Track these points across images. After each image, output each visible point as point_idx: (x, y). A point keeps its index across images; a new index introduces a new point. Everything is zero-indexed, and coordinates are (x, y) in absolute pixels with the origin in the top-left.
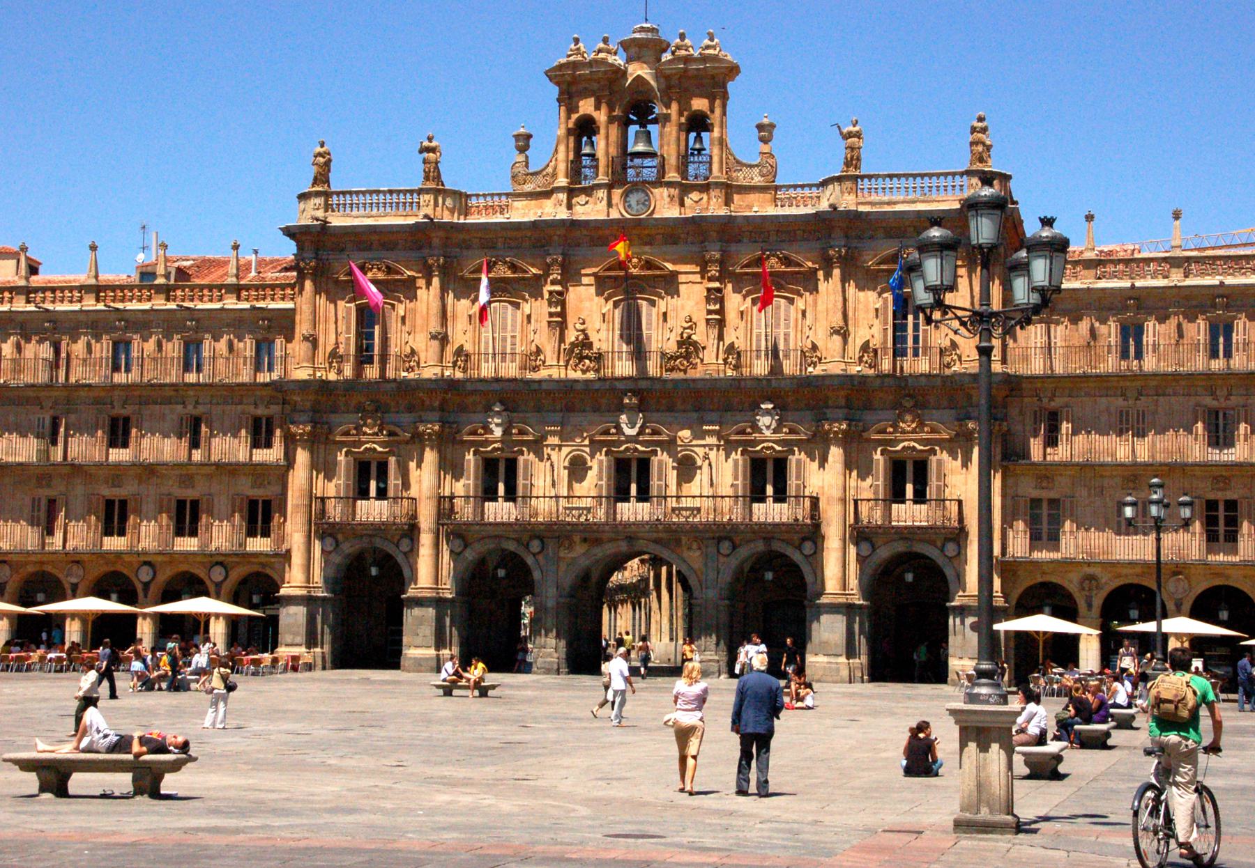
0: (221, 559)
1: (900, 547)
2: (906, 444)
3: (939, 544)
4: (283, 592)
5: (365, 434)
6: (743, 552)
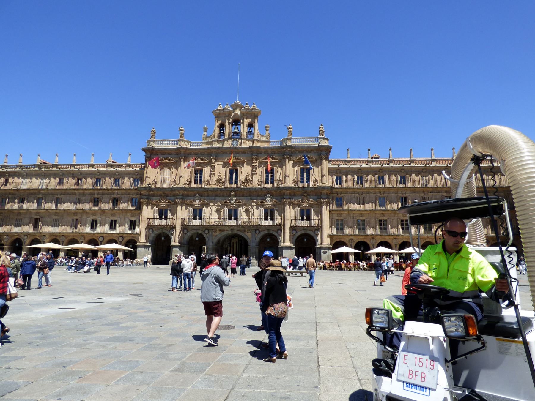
0: (122, 235)
1: (303, 232)
2: (305, 205)
3: (313, 231)
4: (138, 244)
5: (161, 202)
6: (262, 233)
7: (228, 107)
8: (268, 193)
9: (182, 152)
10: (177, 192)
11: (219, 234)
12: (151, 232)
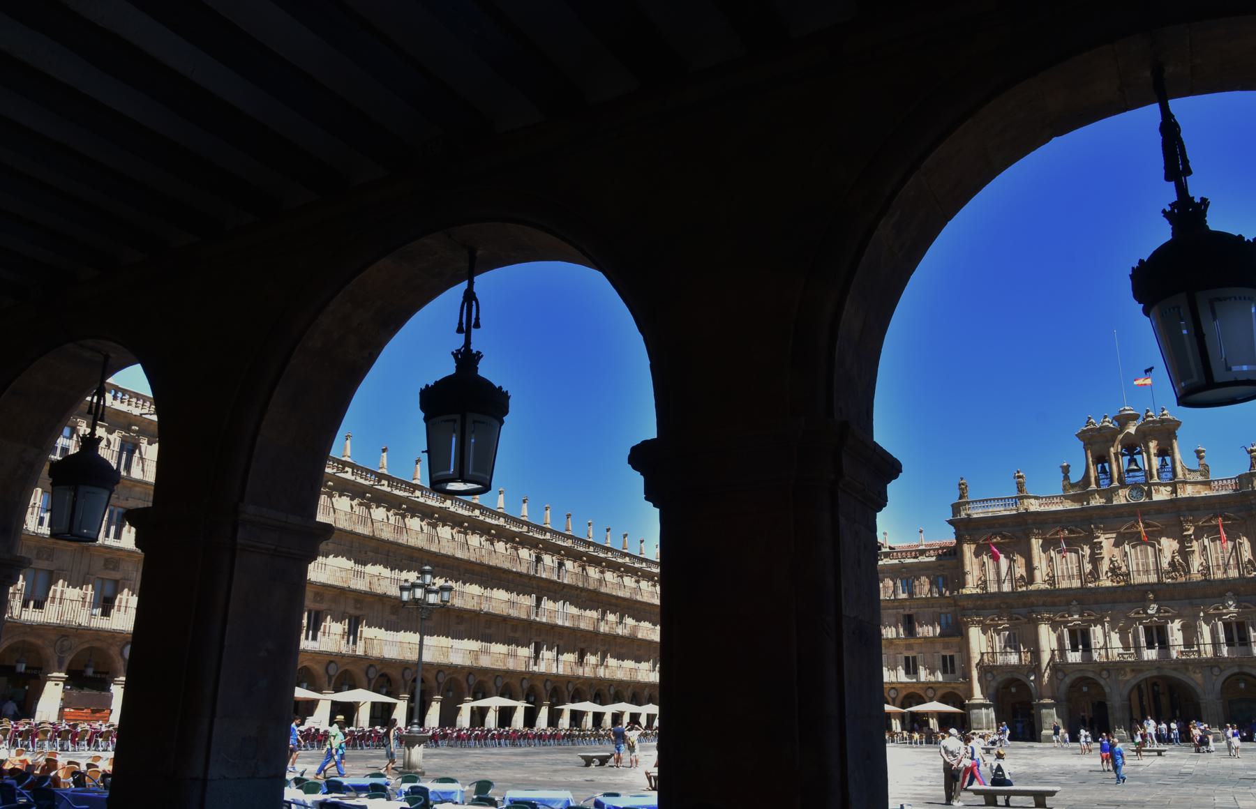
6: (1227, 673)
7: (1109, 423)
8: (1229, 591)
9: (1030, 521)
10: (1032, 599)
11: (1130, 679)
12: (989, 679)
